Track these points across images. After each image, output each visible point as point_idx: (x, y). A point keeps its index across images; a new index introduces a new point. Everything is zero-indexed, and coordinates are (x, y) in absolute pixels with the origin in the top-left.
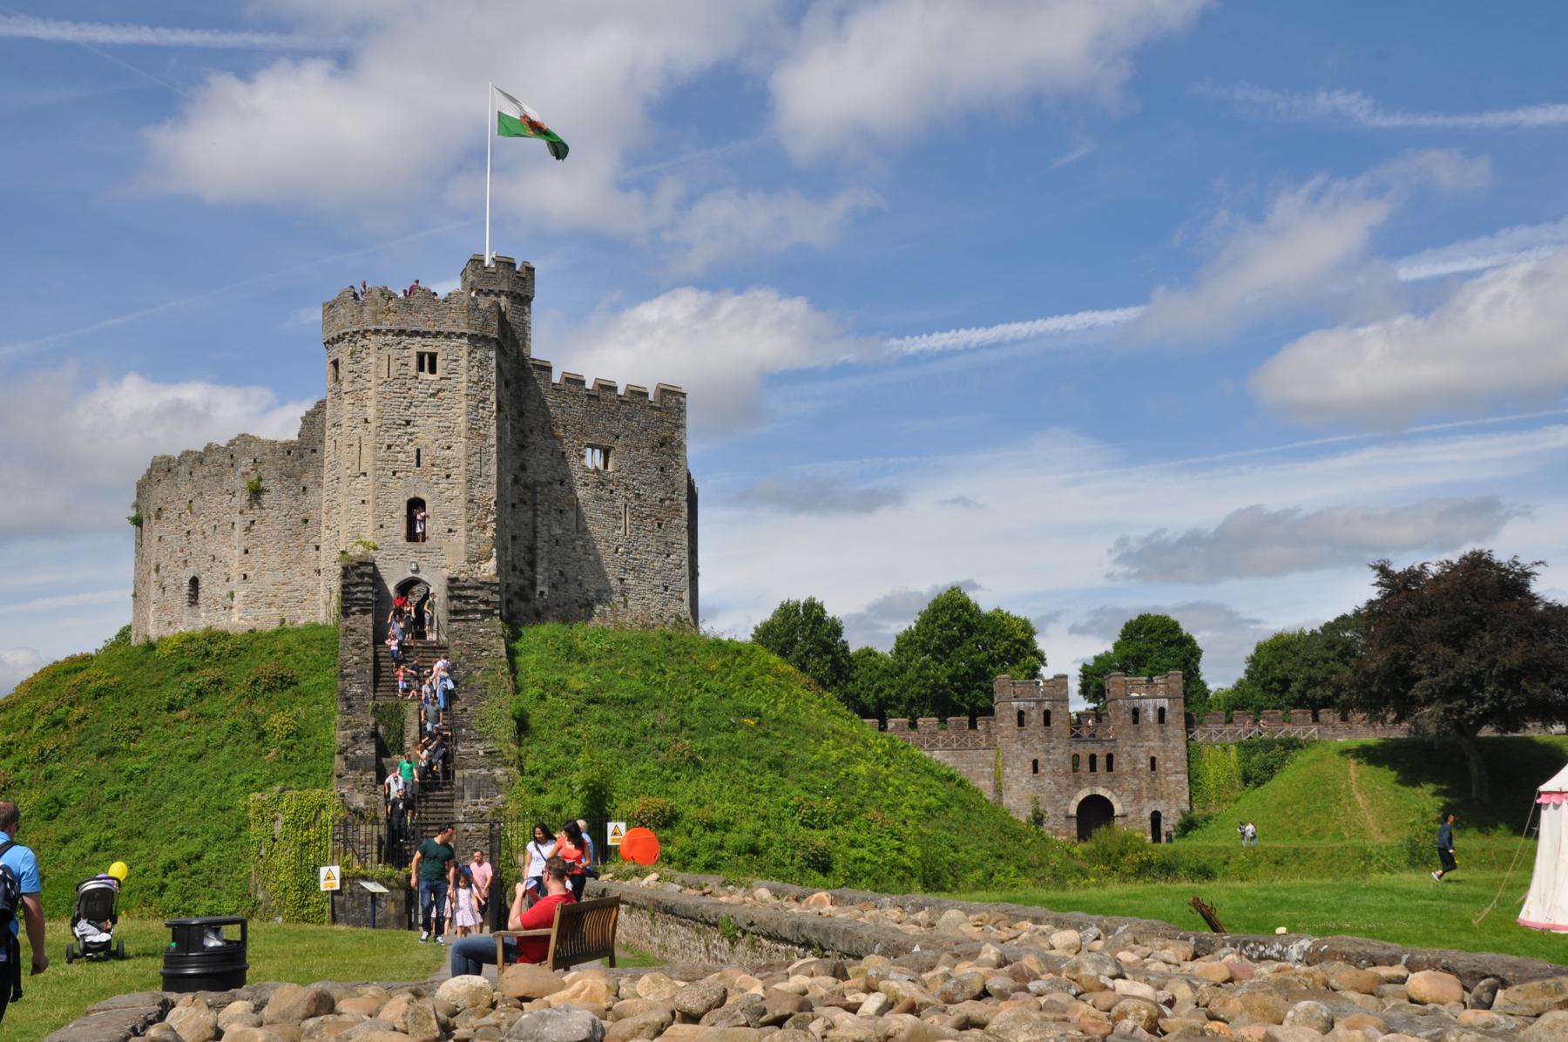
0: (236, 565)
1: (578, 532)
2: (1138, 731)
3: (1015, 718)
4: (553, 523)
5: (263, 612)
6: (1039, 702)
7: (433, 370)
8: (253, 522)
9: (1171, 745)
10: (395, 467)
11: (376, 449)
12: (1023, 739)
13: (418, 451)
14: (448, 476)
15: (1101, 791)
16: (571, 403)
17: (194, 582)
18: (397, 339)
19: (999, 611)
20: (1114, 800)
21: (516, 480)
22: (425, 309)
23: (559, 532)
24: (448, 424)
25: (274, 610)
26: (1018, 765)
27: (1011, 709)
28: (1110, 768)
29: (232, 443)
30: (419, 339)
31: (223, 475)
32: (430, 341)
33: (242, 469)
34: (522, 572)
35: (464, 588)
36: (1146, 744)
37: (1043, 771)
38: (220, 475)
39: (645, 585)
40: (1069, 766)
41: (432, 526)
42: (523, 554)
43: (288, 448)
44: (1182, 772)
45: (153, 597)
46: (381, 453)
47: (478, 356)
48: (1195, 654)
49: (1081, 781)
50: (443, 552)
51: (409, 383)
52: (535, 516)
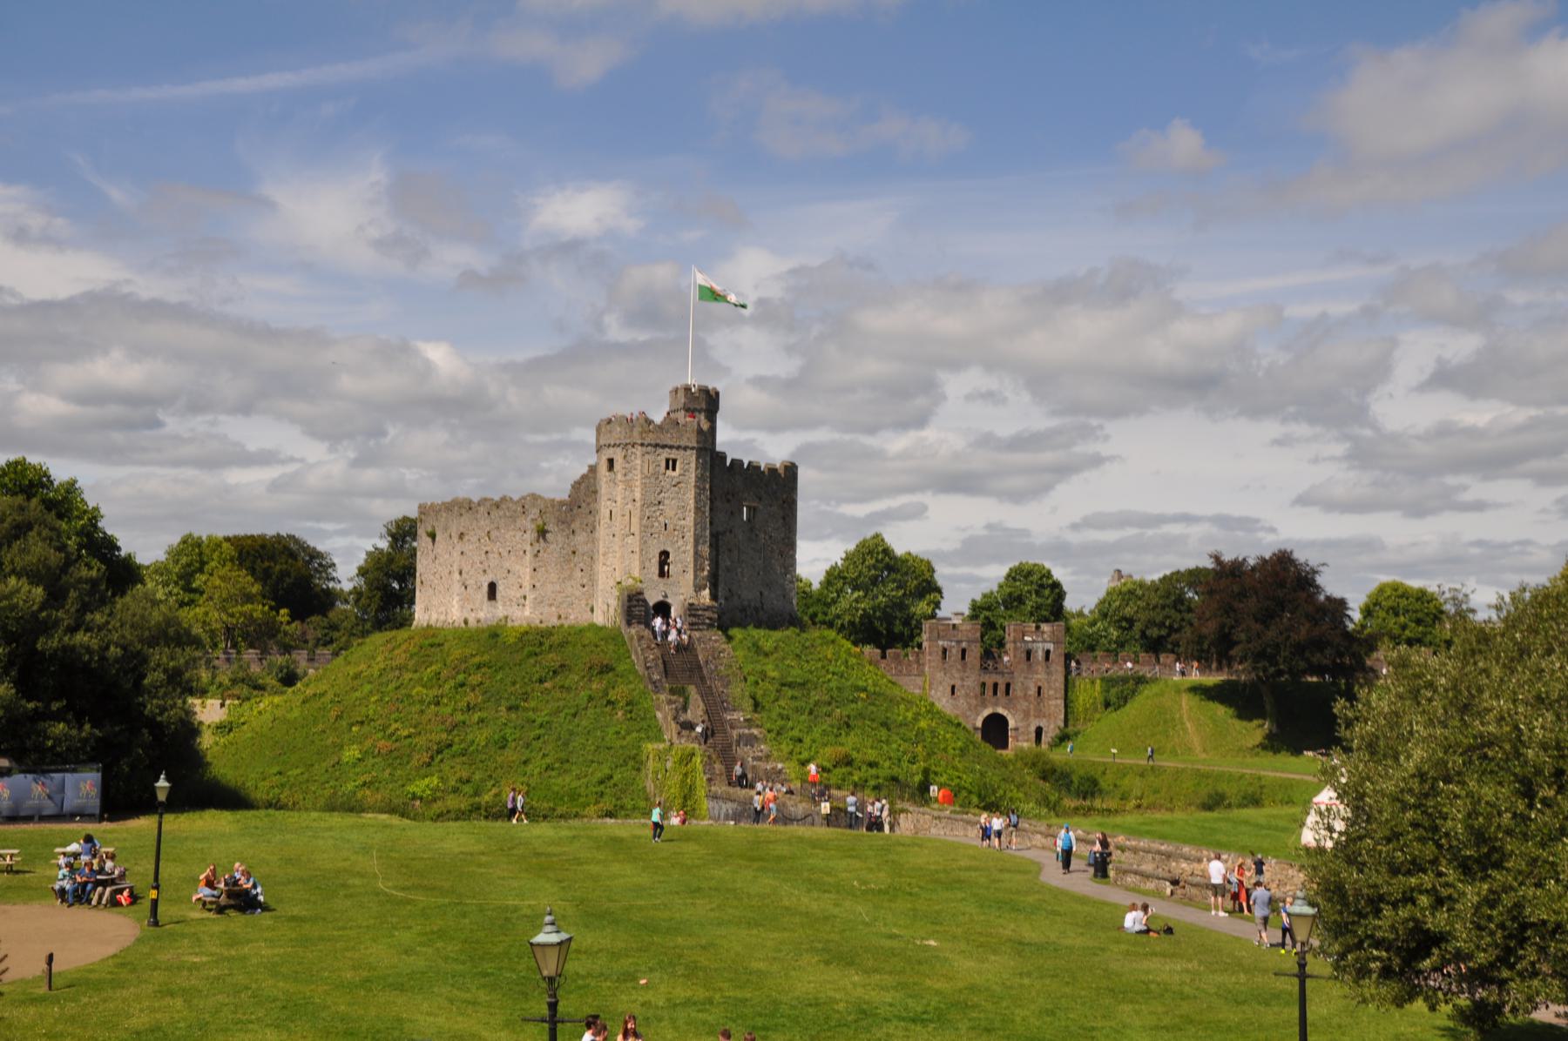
0: (528, 578)
3: (940, 653)
5: (546, 610)
6: (959, 642)
7: (674, 469)
8: (539, 551)
10: (653, 531)
11: (641, 519)
15: (1000, 711)
18: (653, 449)
19: (909, 554)
25: (554, 609)
26: (941, 688)
27: (938, 646)
28: (1007, 693)
32: (674, 451)
35: (697, 610)
38: (513, 519)
40: (978, 690)
41: (673, 569)
51: (661, 477)
52: (717, 555)
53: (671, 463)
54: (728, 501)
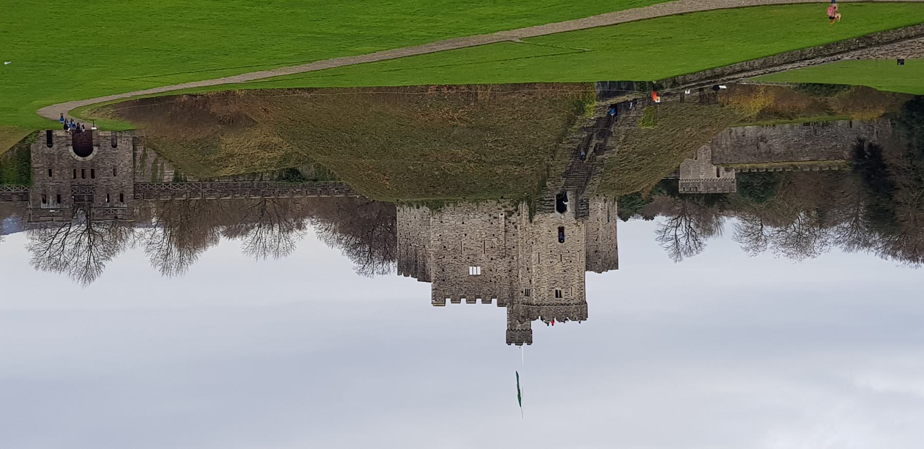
1: (484, 240)
2: (58, 191)
3: (125, 198)
4: (496, 243)
12: (122, 187)
15: (80, 159)
20: (73, 154)
22: (561, 314)
26: (124, 173)
27: (127, 203)
30: (562, 303)
34: (510, 222)
36: (54, 184)
37: (111, 170)
39: (453, 222)
40: (96, 173)
42: (509, 229)
52: (505, 244)
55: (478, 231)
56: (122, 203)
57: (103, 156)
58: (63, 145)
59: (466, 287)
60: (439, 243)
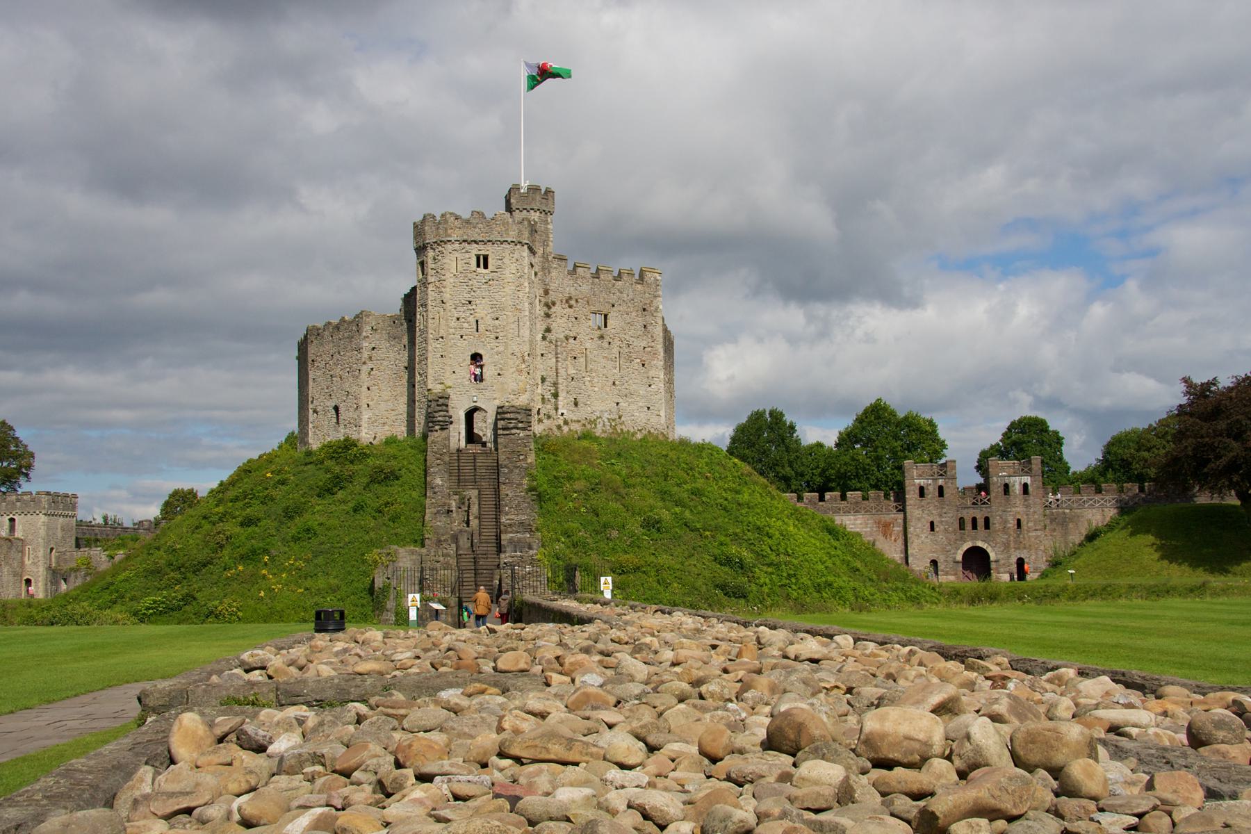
2: (1008, 500)
3: (917, 491)
7: (486, 267)
8: (372, 369)
9: (1032, 510)
13: (477, 321)
14: (497, 338)
15: (980, 544)
16: (581, 284)
17: (336, 409)
20: (989, 550)
21: (544, 338)
22: (480, 225)
23: (575, 372)
24: (495, 302)
25: (386, 428)
26: (920, 525)
27: (914, 485)
28: (987, 526)
29: (357, 316)
30: (476, 246)
31: (352, 338)
32: (481, 246)
33: (364, 334)
39: (633, 407)
40: (957, 526)
43: (394, 320)
44: (1040, 530)
45: (311, 419)
46: (453, 323)
47: (515, 255)
48: (1058, 441)
49: (965, 536)
50: (494, 388)
53: (482, 257)
54: (571, 307)
55: (596, 389)
56: (922, 484)
57: (949, 548)
58: (1003, 562)
59: (614, 294)
60: (651, 374)
